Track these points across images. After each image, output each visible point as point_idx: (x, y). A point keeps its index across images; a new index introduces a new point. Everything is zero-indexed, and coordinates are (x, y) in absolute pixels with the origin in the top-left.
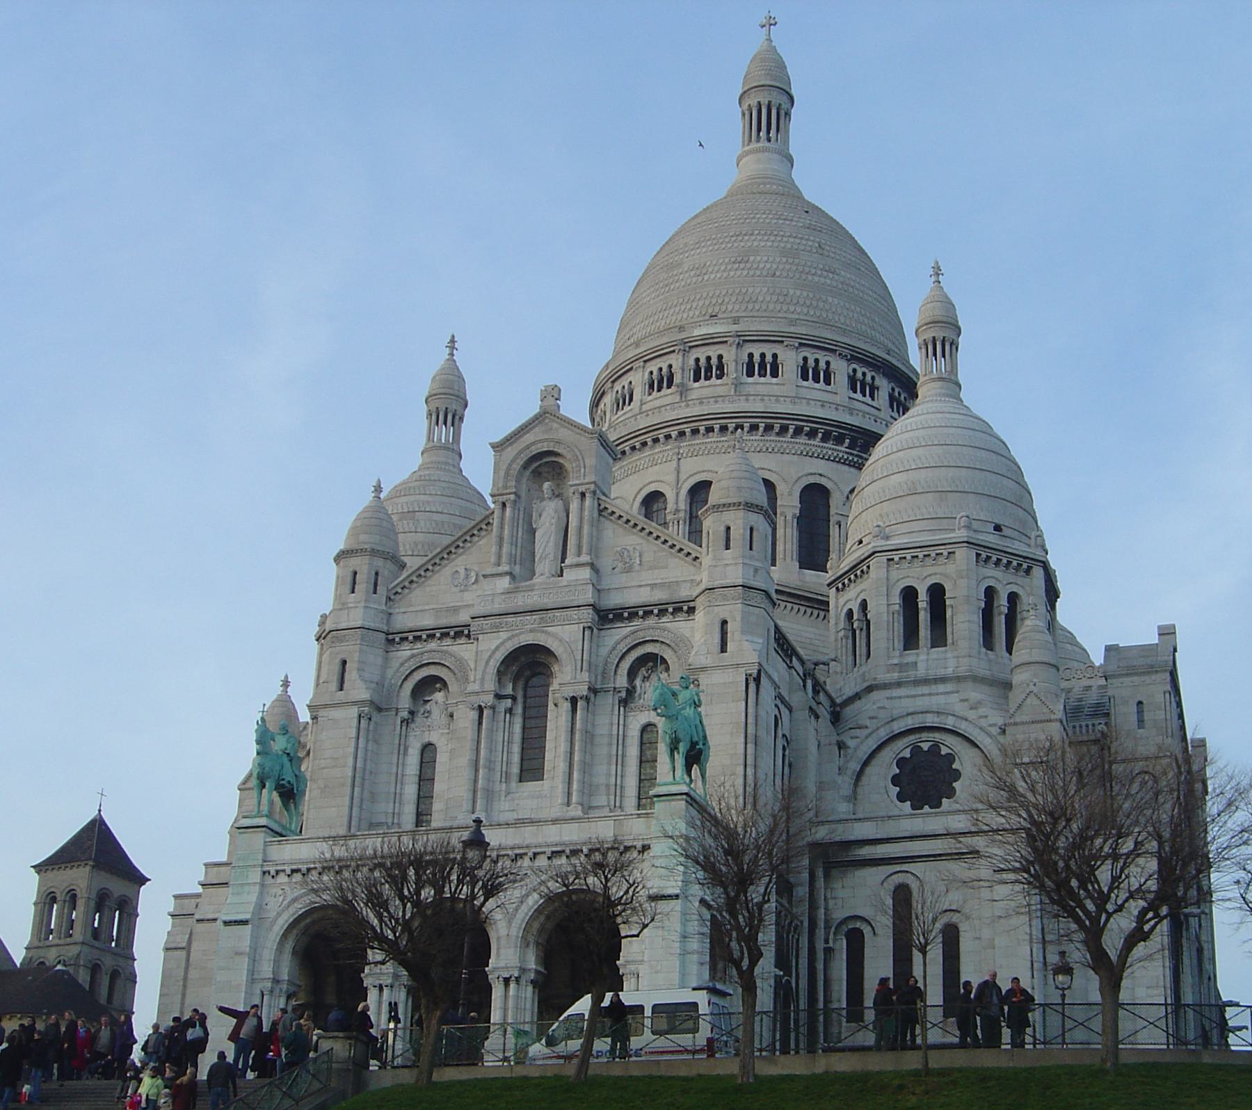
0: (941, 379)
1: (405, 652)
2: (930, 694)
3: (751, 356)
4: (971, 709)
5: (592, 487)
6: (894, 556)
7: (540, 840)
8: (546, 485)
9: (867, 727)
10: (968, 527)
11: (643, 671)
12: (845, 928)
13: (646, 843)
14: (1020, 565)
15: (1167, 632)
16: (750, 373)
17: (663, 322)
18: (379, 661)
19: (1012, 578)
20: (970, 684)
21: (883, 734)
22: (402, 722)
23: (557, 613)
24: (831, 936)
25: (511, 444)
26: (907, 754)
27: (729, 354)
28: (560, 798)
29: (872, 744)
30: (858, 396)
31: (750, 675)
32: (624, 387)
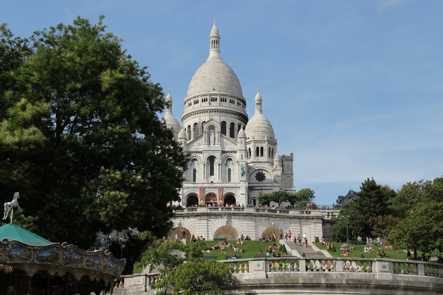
0: (260, 110)
3: (221, 98)
6: (255, 142)
10: (267, 138)
11: (228, 161)
16: (221, 101)
17: (204, 89)
20: (267, 163)
21: (254, 170)
23: (216, 151)
26: (257, 173)
27: (218, 98)
28: (218, 179)
29: (252, 171)
30: (238, 106)
32: (196, 100)
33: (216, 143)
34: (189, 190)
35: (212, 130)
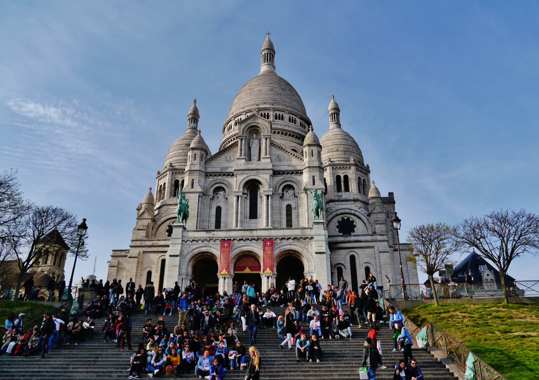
0: (336, 123)
1: (211, 179)
2: (347, 204)
3: (276, 114)
4: (359, 209)
5: (269, 137)
6: (334, 166)
7: (277, 234)
8: (254, 135)
9: (329, 212)
10: (354, 161)
12: (337, 267)
13: (312, 236)
14: (365, 172)
15: (391, 194)
16: (276, 119)
17: (250, 104)
18: (204, 181)
19: (363, 175)
21: (334, 214)
22: (210, 199)
23: (262, 171)
24: (333, 269)
25: (244, 123)
26: (340, 220)
28: (265, 225)
29: (331, 216)
30: (302, 128)
31: (323, 192)
32: (238, 119)
33: (263, 155)
34: (197, 246)
35: (254, 135)
